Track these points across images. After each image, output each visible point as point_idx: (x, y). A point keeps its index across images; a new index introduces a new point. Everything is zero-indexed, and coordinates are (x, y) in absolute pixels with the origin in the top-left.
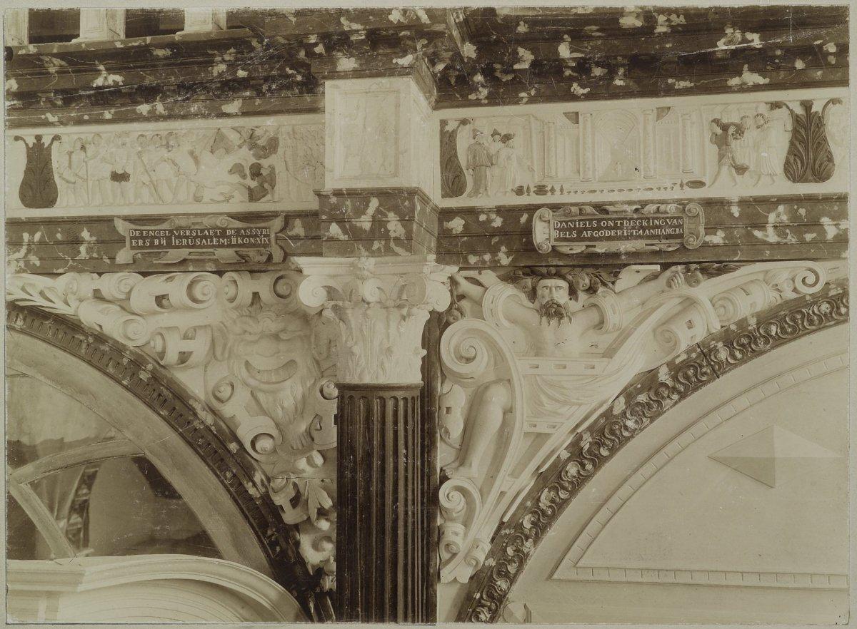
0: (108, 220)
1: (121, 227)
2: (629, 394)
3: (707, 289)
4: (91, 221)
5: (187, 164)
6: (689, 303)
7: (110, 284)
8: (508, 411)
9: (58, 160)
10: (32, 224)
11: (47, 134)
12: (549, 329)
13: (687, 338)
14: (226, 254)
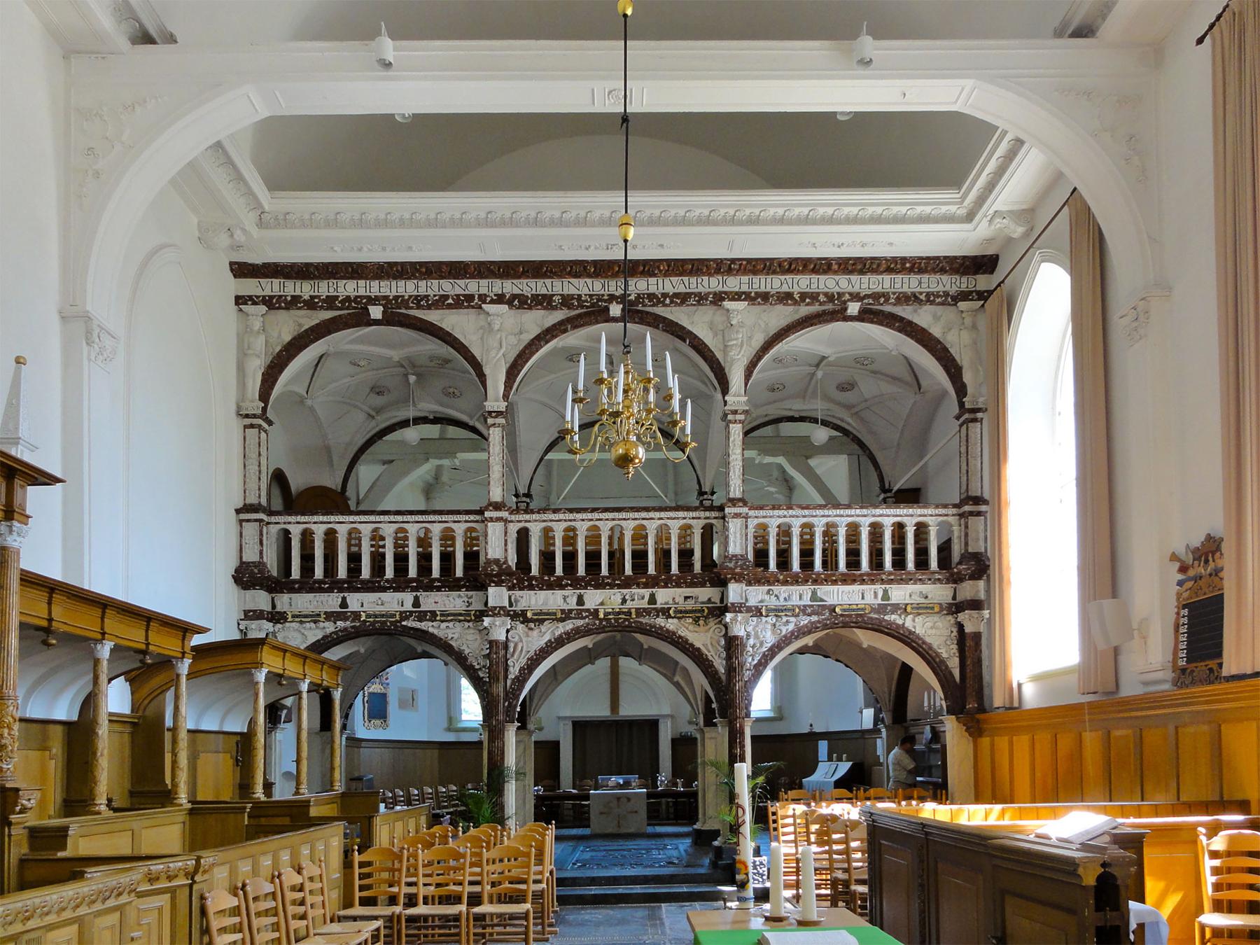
0: (435, 611)
1: (438, 613)
2: (546, 643)
3: (561, 625)
4: (430, 611)
5: (452, 600)
6: (558, 627)
7: (434, 624)
8: (522, 647)
9: (421, 599)
10: (415, 612)
11: (418, 594)
12: (530, 632)
13: (557, 633)
14: (462, 618)
